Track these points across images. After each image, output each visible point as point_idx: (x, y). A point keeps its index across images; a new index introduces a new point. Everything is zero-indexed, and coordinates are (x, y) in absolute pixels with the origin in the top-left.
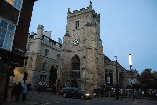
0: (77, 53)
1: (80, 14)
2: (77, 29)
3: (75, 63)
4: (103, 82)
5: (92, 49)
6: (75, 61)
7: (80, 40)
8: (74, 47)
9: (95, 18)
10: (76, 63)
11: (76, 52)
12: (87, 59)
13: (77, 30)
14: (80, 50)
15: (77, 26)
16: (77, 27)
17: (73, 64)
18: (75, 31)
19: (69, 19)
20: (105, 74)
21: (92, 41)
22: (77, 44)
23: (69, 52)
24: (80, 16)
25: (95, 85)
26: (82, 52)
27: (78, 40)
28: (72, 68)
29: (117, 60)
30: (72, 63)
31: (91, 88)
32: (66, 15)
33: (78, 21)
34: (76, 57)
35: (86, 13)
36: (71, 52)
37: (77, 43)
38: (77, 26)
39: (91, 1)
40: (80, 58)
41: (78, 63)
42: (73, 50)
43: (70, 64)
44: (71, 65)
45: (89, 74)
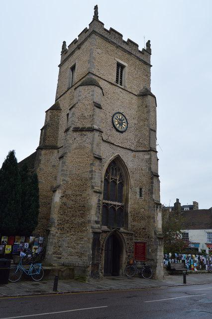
10: (114, 182)
11: (119, 148)
14: (128, 149)
22: (123, 130)
26: (134, 157)
33: (123, 67)
34: (117, 164)
36: (107, 144)
39: (149, 41)
41: (118, 182)
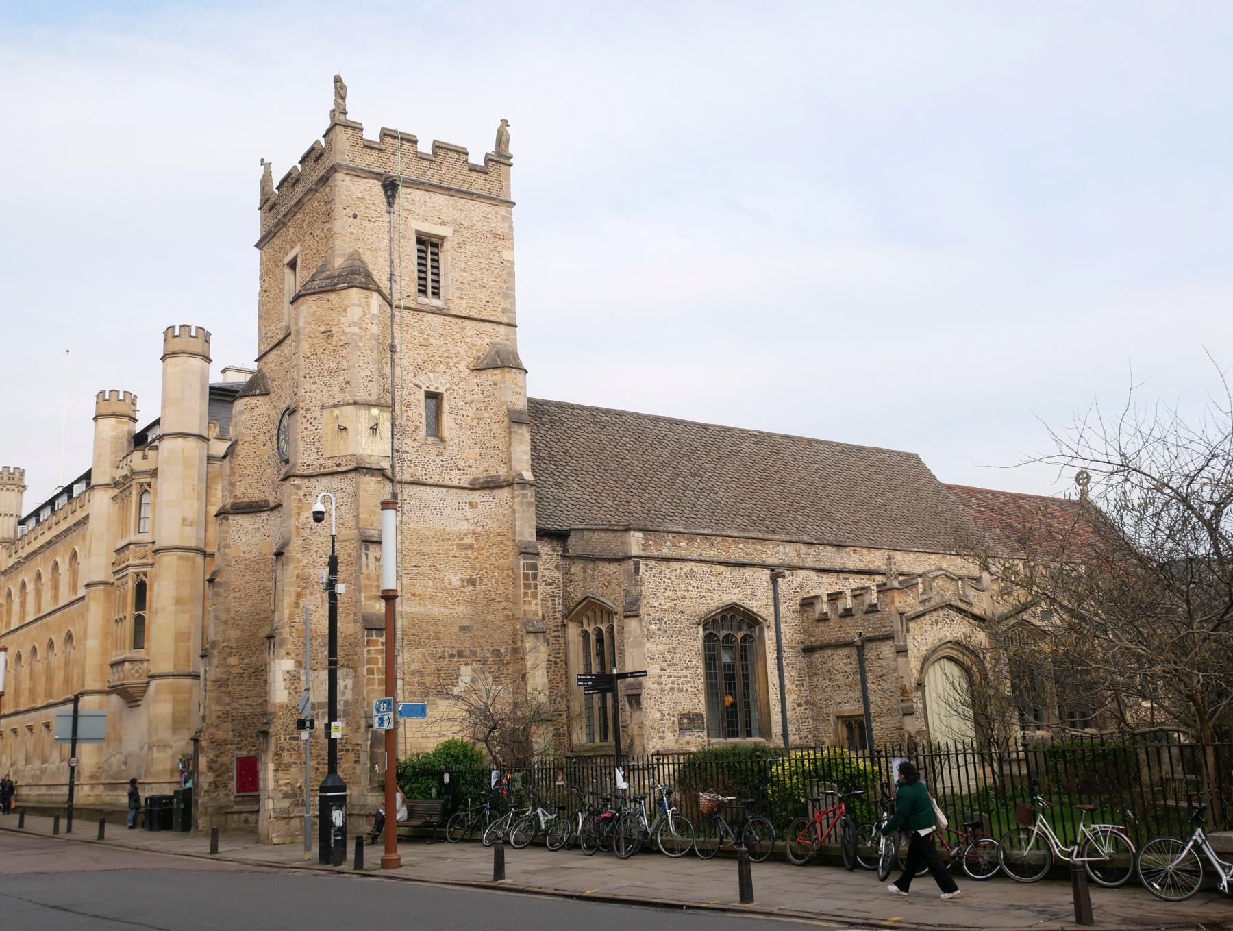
5: (336, 478)
12: (305, 562)
21: (336, 412)
23: (264, 515)
32: (252, 224)
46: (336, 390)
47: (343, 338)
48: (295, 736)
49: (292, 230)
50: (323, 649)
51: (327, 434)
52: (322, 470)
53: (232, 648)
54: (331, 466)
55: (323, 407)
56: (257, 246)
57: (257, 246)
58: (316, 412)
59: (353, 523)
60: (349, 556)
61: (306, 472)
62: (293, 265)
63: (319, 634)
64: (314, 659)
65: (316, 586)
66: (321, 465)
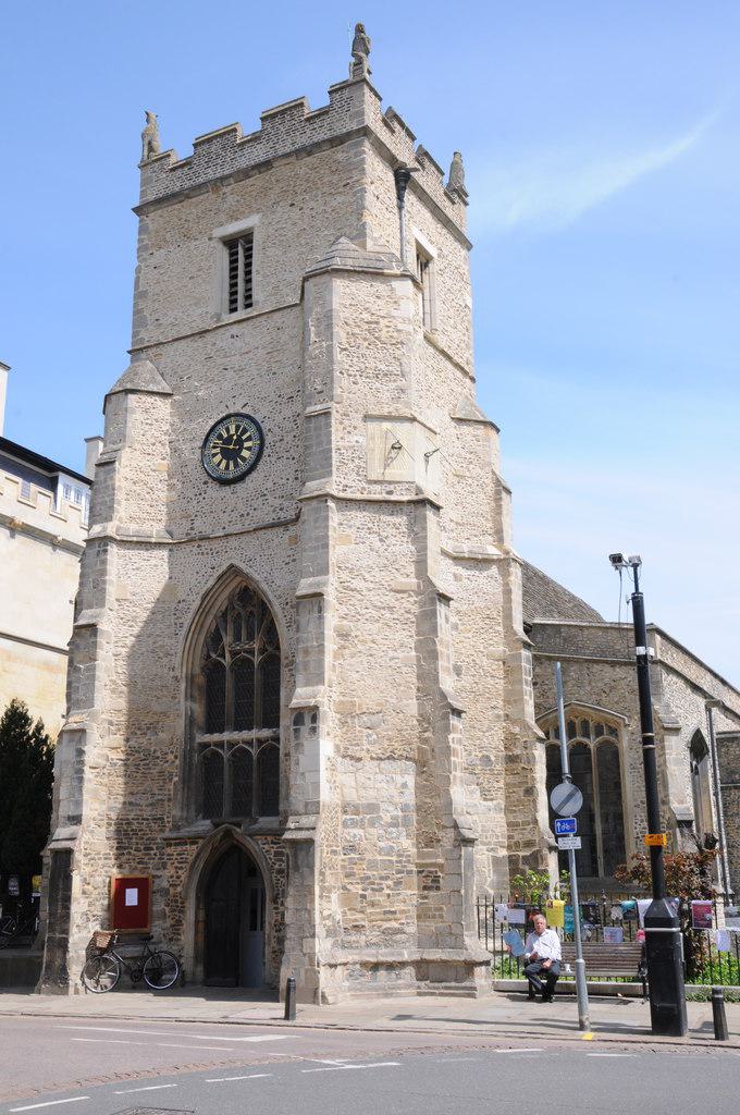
0: (236, 554)
1: (266, 165)
2: (241, 314)
3: (227, 661)
4: (529, 844)
6: (227, 639)
7: (265, 427)
8: (214, 491)
9: (409, 197)
10: (243, 665)
11: (233, 542)
13: (235, 330)
14: (272, 526)
15: (239, 292)
16: (233, 293)
17: (213, 671)
18: (222, 339)
19: (155, 218)
20: (540, 753)
21: (386, 425)
22: (243, 467)
24: (257, 180)
25: (436, 880)
27: (253, 421)
28: (198, 709)
29: (637, 604)
30: (197, 662)
31: (398, 907)
33: (247, 237)
35: (318, 146)
37: (245, 453)
38: (239, 292)
40: (277, 608)
41: (257, 660)
42: (207, 531)
43: (181, 672)
44: (191, 680)
45: (370, 765)
46: (385, 396)
47: (395, 334)
48: (334, 848)
49: (230, 199)
50: (370, 732)
51: (373, 450)
52: (365, 496)
53: (111, 723)
54: (378, 493)
55: (367, 418)
56: (137, 210)
57: (137, 210)
58: (357, 419)
59: (412, 569)
60: (408, 612)
61: (341, 495)
62: (239, 246)
63: (364, 710)
64: (358, 745)
65: (360, 647)
66: (364, 488)
